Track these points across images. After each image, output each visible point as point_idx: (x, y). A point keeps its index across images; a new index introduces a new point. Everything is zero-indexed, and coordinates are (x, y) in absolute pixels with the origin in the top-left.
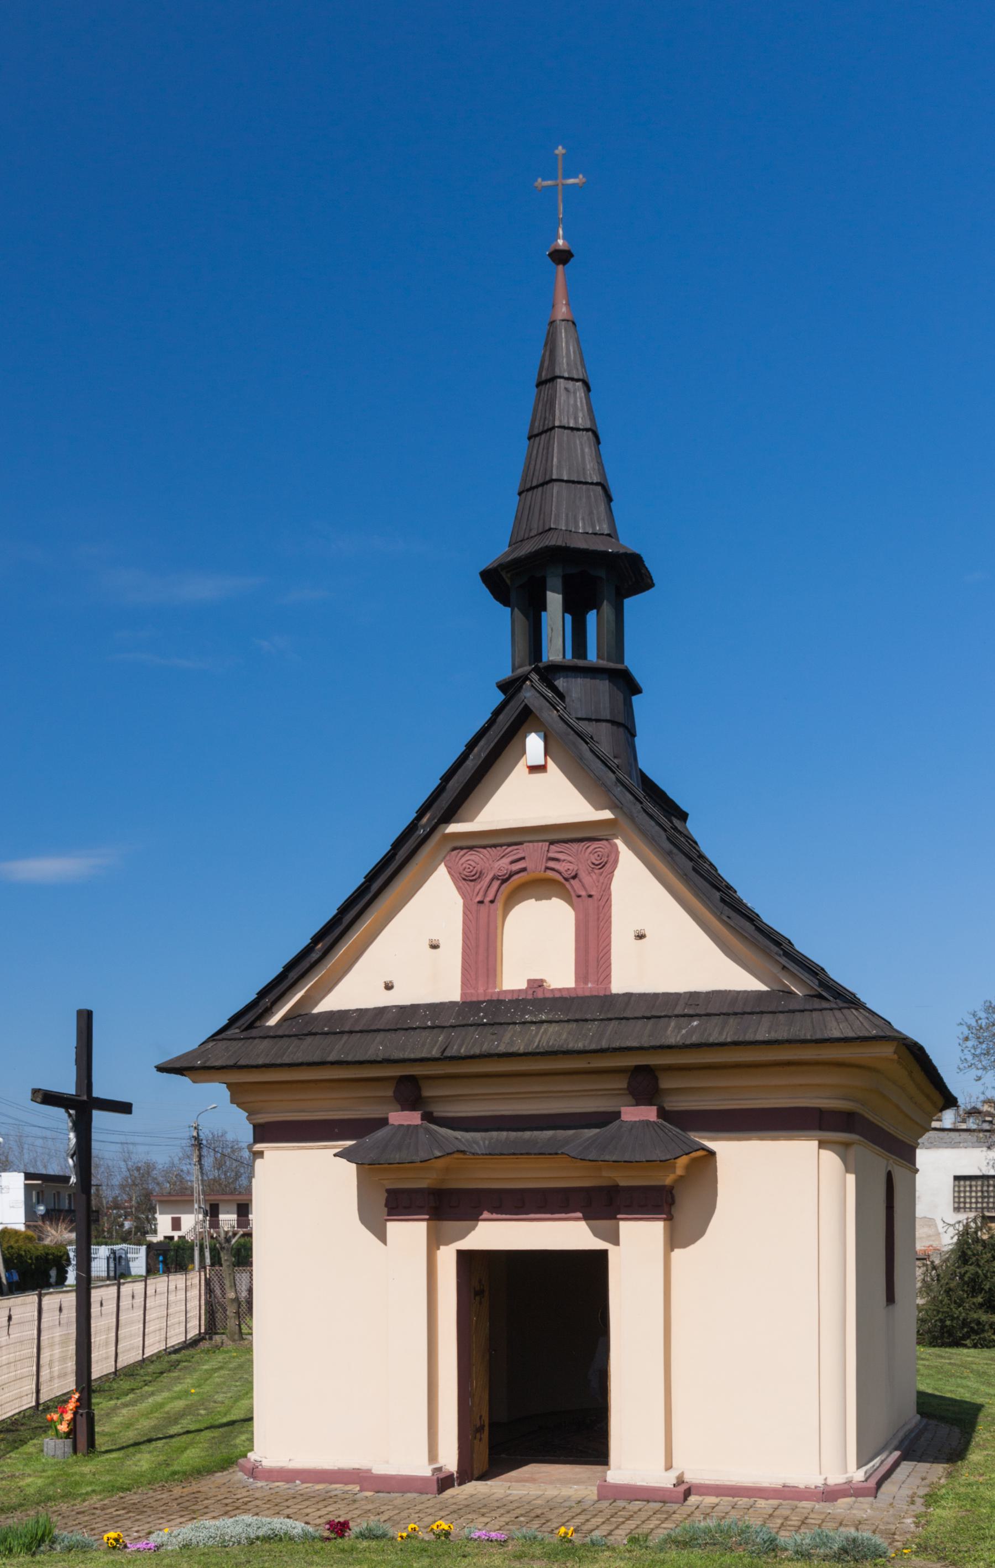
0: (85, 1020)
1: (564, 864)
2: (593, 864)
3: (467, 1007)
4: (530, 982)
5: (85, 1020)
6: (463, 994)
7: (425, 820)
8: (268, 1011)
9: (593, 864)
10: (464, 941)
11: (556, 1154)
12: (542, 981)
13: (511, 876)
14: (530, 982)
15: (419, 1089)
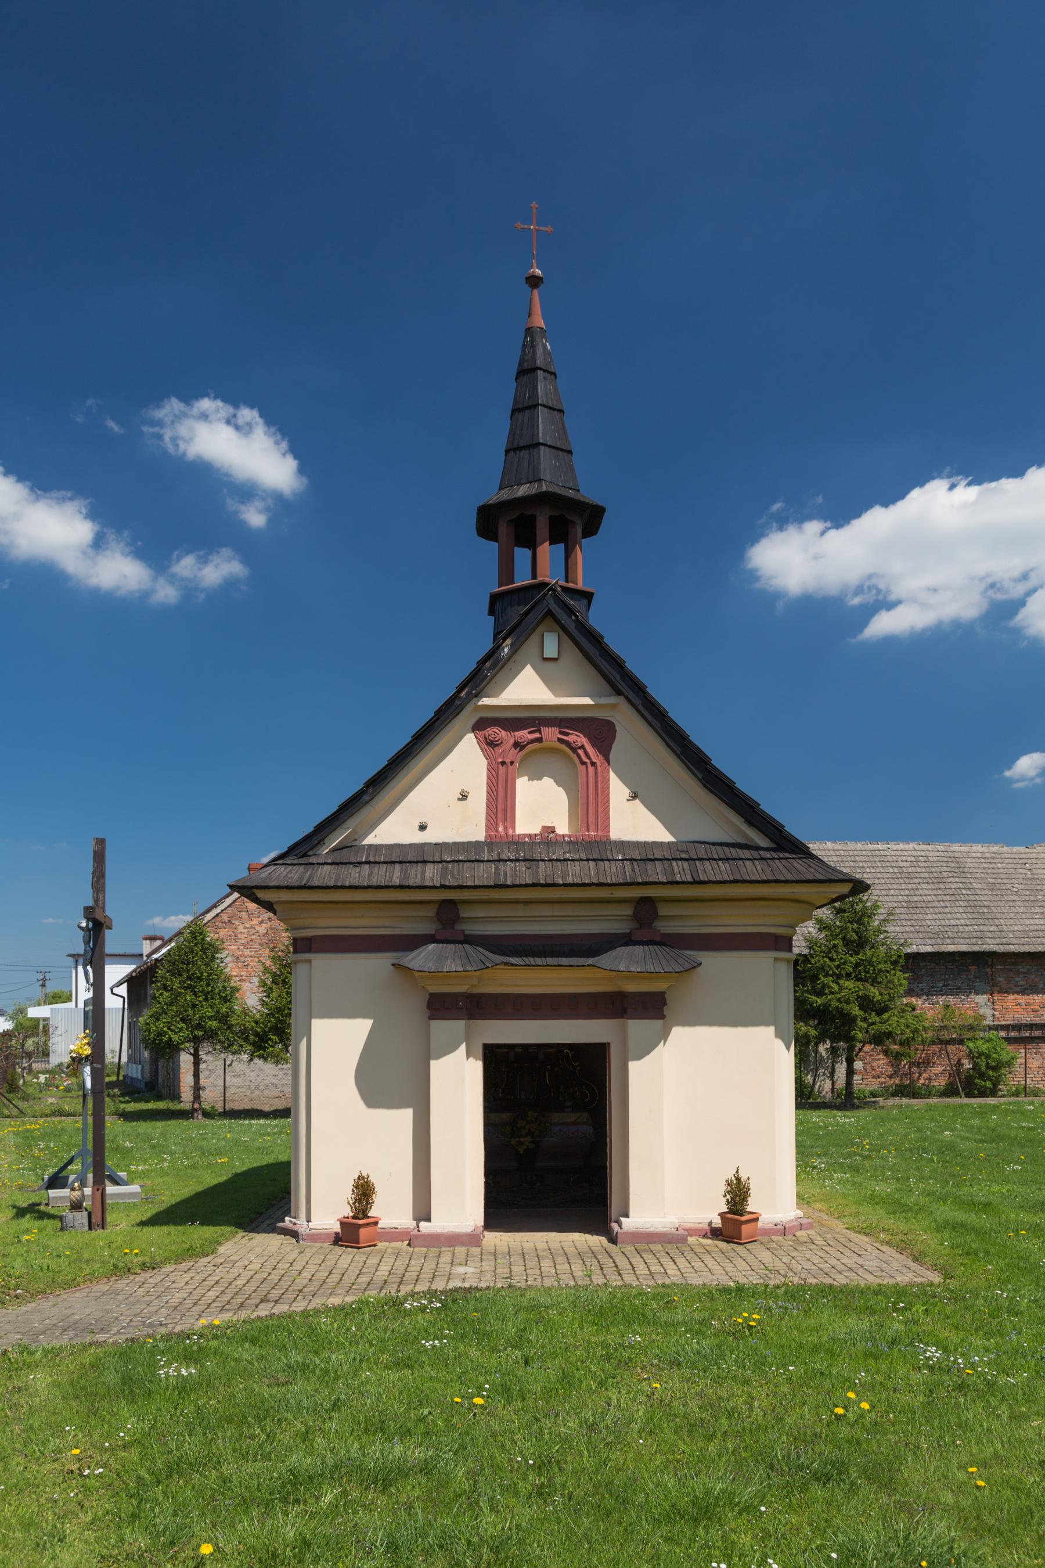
0: (101, 842)
1: (572, 736)
2: (595, 738)
3: (489, 843)
4: (544, 828)
5: (101, 842)
6: (487, 837)
7: (463, 694)
8: (321, 842)
9: (595, 738)
10: (488, 792)
11: (583, 966)
12: (554, 827)
13: (528, 744)
14: (544, 828)
15: (457, 912)
